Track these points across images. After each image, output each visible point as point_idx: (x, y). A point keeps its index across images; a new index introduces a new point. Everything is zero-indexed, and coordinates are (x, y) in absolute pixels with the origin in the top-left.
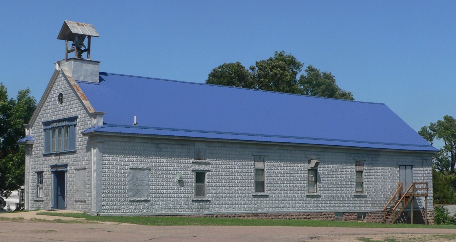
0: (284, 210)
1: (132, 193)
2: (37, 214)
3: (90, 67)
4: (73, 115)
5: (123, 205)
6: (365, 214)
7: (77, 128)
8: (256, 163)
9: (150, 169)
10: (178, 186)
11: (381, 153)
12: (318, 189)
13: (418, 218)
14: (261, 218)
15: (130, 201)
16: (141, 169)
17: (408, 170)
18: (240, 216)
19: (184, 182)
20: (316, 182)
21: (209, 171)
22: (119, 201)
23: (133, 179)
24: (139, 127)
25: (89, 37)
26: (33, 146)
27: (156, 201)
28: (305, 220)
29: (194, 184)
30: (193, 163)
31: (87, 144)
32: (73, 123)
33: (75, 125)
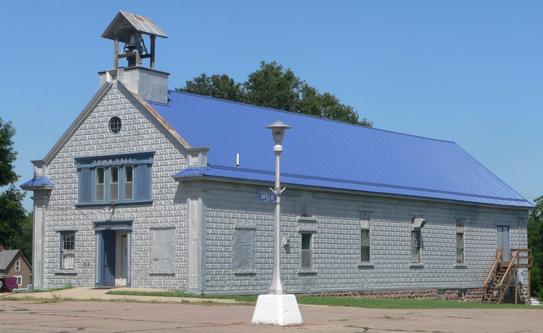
0: (388, 286)
1: (237, 263)
2: (107, 293)
3: (157, 80)
4: (145, 149)
5: (228, 280)
6: (465, 291)
7: (154, 168)
8: (362, 221)
9: (255, 230)
10: (284, 253)
11: (481, 210)
12: (421, 257)
13: (510, 297)
14: (367, 297)
15: (236, 275)
16: (247, 229)
17: (505, 233)
18: (346, 295)
19: (290, 247)
20: (419, 248)
21: (315, 232)
22: (224, 274)
23: (238, 243)
24: (241, 170)
25: (153, 37)
26: (52, 194)
27: (261, 274)
28: (409, 299)
29: (300, 250)
30: (300, 221)
31: (177, 193)
32: (146, 161)
33: (150, 165)
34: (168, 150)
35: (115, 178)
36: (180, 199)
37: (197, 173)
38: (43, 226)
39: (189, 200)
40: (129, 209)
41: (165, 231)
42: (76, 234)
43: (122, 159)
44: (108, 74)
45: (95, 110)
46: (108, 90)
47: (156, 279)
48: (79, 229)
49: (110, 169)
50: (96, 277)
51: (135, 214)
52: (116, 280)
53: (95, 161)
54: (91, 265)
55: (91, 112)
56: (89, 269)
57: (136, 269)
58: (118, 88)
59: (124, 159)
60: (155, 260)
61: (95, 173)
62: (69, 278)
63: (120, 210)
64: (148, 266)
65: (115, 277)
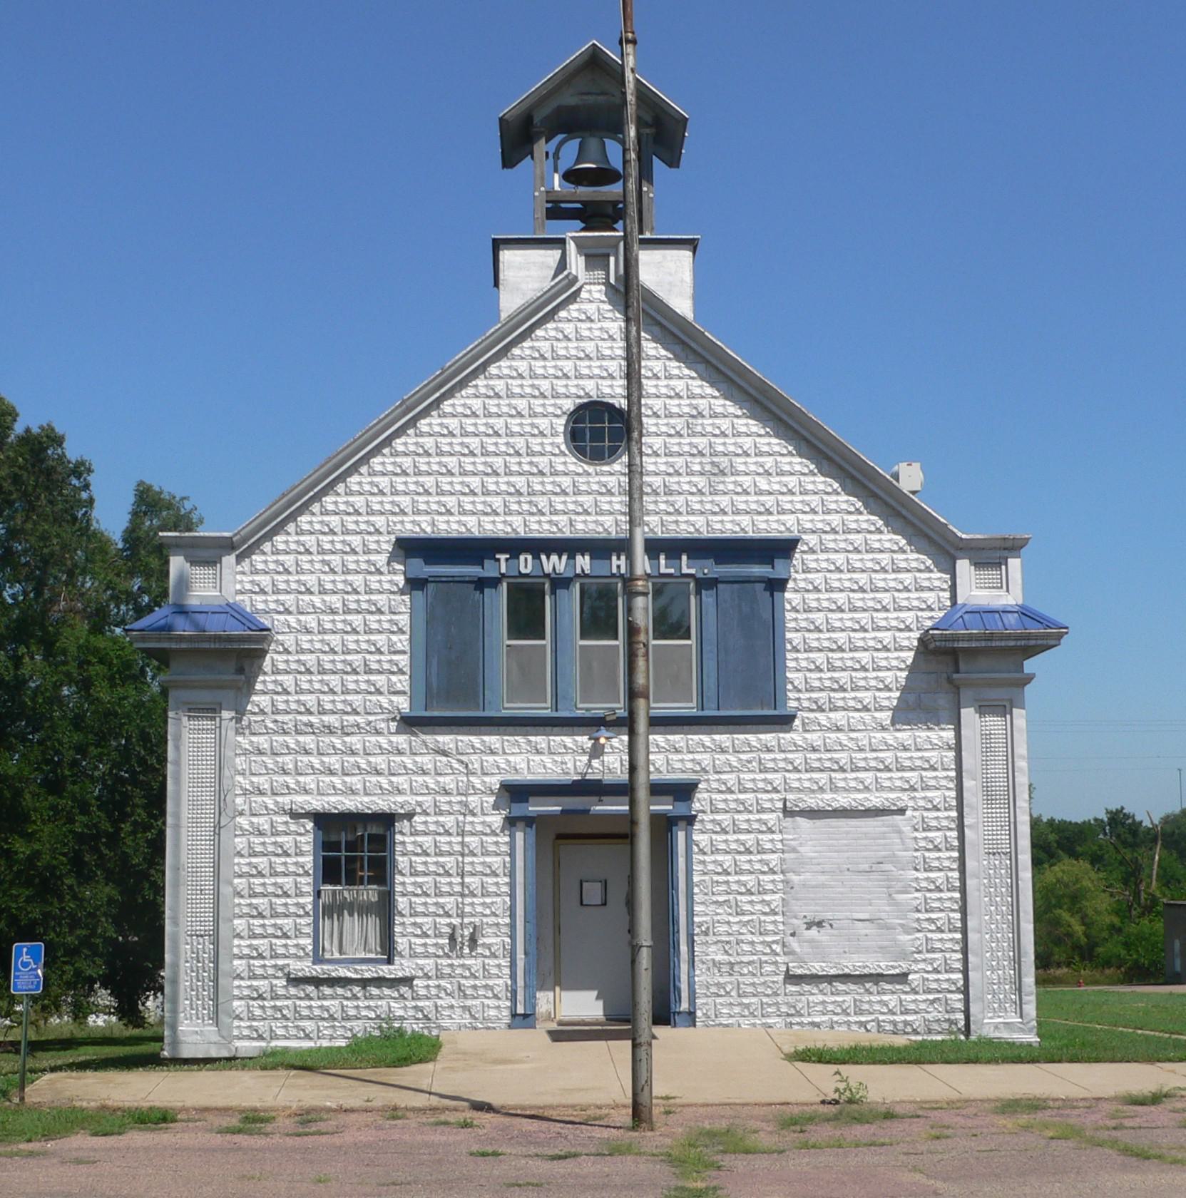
31: (905, 690)
32: (758, 570)
33: (777, 585)
36: (915, 707)
47: (815, 995)
50: (514, 993)
51: (705, 759)
53: (503, 557)
54: (489, 947)
55: (474, 375)
57: (720, 957)
60: (809, 926)
61: (499, 600)
62: (371, 997)
64: (777, 948)
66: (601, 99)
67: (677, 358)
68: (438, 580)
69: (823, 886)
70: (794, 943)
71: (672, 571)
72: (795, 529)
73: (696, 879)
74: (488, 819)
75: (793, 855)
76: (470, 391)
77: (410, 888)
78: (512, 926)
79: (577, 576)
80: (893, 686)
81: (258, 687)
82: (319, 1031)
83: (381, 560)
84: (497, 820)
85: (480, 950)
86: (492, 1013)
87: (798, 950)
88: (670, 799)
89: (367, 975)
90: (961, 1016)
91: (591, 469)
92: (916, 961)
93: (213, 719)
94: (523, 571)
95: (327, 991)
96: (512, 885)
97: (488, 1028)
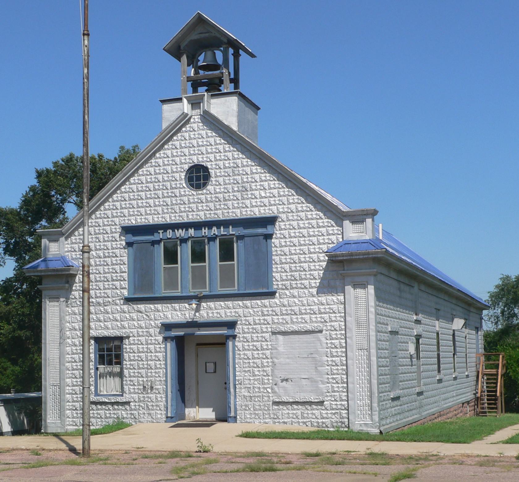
4: (258, 212)
31: (322, 279)
32: (260, 231)
33: (269, 237)
34: (303, 215)
35: (198, 256)
36: (328, 286)
37: (353, 249)
38: (62, 330)
39: (349, 289)
40: (230, 303)
41: (301, 336)
42: (126, 341)
43: (214, 228)
44: (185, 100)
45: (158, 155)
46: (184, 125)
47: (285, 410)
48: (131, 335)
49: (189, 243)
50: (167, 408)
51: (240, 311)
52: (187, 410)
53: (161, 231)
54: (157, 389)
55: (150, 158)
56: (153, 396)
58: (202, 122)
59: (219, 228)
60: (282, 381)
62: (115, 409)
63: (212, 304)
64: (269, 390)
65: (185, 407)
66: (207, 35)
67: (229, 143)
68: (138, 242)
69: (289, 364)
70: (276, 388)
71: (226, 233)
72: (276, 212)
73: (236, 361)
74: (157, 338)
75: (275, 351)
76: (149, 164)
77: (128, 366)
78: (166, 381)
79: (189, 237)
80: (317, 277)
81: (74, 288)
82: (97, 423)
83: (117, 235)
84: (160, 338)
85: (154, 391)
86: (159, 416)
87: (278, 391)
88: (226, 328)
89: (113, 401)
90: (346, 420)
91: (195, 193)
92: (327, 396)
93: (58, 301)
94: (169, 237)
95: (99, 407)
96: (166, 364)
97: (247, 422)
